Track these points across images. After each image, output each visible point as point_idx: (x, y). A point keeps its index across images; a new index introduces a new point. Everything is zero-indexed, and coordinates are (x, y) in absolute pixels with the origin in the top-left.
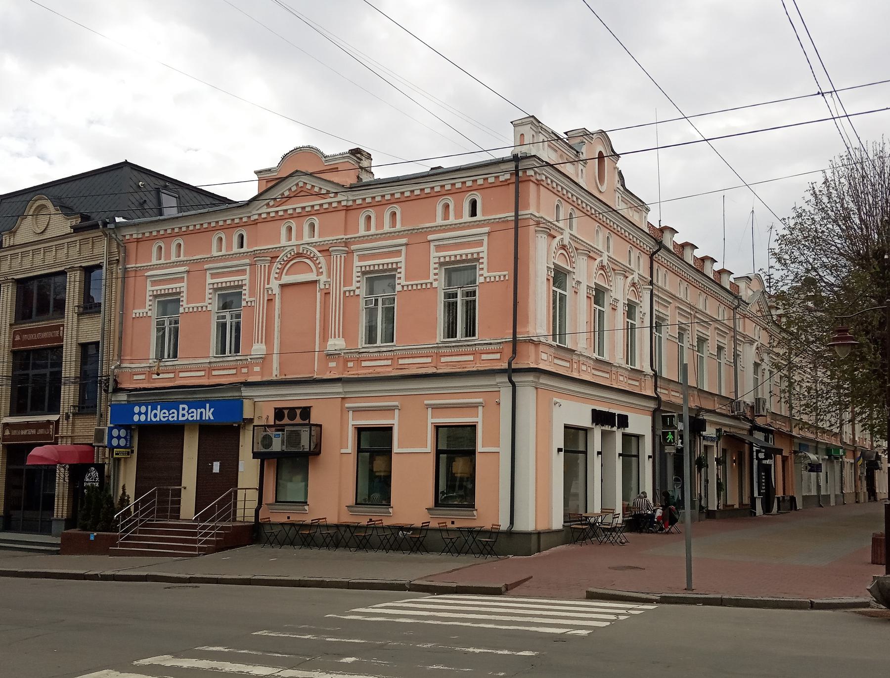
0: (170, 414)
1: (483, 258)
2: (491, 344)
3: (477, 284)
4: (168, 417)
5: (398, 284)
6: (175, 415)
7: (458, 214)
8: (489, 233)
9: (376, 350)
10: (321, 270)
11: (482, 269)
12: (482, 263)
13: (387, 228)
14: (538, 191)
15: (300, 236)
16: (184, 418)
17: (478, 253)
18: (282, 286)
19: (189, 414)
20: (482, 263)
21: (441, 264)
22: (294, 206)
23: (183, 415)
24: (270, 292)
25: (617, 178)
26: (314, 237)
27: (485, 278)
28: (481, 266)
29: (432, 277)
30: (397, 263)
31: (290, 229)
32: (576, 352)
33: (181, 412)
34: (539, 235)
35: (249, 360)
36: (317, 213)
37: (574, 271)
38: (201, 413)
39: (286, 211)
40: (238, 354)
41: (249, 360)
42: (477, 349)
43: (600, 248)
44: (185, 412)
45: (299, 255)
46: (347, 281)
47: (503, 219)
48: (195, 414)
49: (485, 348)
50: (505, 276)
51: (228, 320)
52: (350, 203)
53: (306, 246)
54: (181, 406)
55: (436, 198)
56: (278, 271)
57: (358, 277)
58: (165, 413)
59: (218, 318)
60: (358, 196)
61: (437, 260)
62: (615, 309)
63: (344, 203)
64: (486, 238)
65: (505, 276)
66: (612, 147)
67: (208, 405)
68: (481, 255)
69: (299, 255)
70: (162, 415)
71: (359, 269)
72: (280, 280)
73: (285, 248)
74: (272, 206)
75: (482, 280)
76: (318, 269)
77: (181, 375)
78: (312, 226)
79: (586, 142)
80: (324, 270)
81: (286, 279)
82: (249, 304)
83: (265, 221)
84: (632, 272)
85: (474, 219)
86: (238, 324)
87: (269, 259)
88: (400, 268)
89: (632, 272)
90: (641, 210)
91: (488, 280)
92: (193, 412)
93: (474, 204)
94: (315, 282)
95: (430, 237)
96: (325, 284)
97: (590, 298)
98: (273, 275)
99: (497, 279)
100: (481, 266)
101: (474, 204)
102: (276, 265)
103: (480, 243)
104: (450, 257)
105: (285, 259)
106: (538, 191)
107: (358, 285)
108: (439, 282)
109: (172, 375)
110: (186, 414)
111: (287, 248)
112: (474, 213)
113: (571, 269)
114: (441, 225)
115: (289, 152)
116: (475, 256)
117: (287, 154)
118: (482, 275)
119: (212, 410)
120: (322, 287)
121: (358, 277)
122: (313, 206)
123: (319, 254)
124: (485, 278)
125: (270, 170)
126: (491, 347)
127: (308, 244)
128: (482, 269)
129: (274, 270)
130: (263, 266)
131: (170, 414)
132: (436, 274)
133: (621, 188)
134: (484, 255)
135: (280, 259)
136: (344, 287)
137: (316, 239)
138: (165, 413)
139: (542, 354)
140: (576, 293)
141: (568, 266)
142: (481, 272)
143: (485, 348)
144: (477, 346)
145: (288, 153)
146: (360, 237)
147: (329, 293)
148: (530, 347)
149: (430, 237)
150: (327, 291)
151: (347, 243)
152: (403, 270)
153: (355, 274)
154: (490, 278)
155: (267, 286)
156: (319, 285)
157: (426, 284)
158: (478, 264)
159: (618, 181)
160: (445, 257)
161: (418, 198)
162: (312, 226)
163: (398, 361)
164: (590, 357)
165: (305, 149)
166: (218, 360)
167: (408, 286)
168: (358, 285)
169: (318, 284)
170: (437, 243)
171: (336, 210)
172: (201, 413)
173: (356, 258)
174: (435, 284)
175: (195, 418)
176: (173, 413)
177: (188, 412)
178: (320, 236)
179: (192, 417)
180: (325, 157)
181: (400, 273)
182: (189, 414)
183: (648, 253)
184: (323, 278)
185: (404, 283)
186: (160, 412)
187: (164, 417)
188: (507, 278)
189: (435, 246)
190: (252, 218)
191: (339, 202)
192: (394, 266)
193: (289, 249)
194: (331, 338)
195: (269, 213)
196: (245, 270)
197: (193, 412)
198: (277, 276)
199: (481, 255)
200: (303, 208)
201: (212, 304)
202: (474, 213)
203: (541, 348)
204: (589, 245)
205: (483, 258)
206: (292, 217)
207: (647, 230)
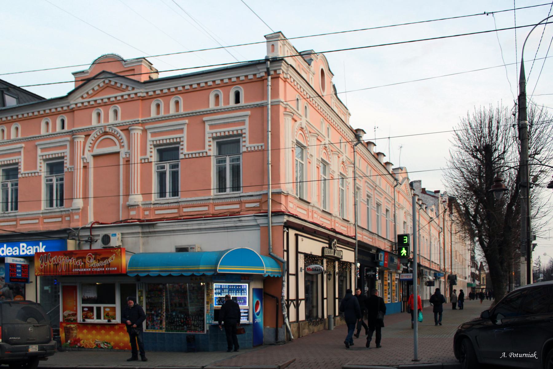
0: (13, 250)
1: (245, 133)
2: (252, 196)
4: (12, 252)
5: (182, 153)
6: (18, 251)
10: (122, 144)
11: (245, 141)
12: (245, 137)
13: (172, 111)
14: (285, 86)
15: (107, 119)
16: (24, 253)
17: (241, 130)
18: (95, 156)
19: (27, 250)
20: (245, 137)
21: (214, 139)
23: (23, 251)
28: (244, 139)
29: (207, 148)
30: (180, 138)
31: (99, 115)
33: (22, 249)
35: (71, 211)
36: (119, 102)
38: (36, 249)
39: (95, 101)
40: (62, 207)
41: (71, 211)
42: (242, 200)
44: (24, 249)
45: (106, 133)
48: (31, 250)
50: (262, 146)
51: (54, 182)
52: (145, 94)
54: (21, 245)
55: (209, 90)
56: (91, 145)
58: (9, 250)
59: (47, 181)
60: (150, 89)
61: (211, 135)
67: (41, 244)
68: (244, 131)
69: (106, 133)
70: (8, 251)
71: (152, 143)
72: (92, 152)
75: (244, 149)
76: (120, 143)
77: (22, 222)
78: (116, 112)
80: (125, 143)
82: (70, 171)
83: (80, 109)
85: (238, 105)
86: (62, 185)
87: (84, 136)
91: (249, 149)
92: (30, 249)
93: (237, 95)
94: (118, 153)
95: (205, 118)
96: (126, 155)
98: (87, 148)
99: (256, 148)
100: (244, 139)
101: (237, 95)
102: (90, 140)
103: (243, 123)
104: (220, 133)
105: (96, 136)
106: (285, 86)
108: (212, 150)
109: (14, 223)
110: (26, 250)
114: (213, 109)
116: (239, 132)
118: (245, 146)
119: (44, 247)
120: (124, 156)
122: (116, 97)
123: (121, 133)
126: (252, 198)
128: (245, 141)
129: (88, 145)
130: (79, 142)
131: (13, 250)
135: (92, 136)
137: (119, 120)
138: (9, 250)
142: (244, 144)
144: (242, 198)
149: (205, 118)
150: (127, 159)
151: (143, 123)
152: (185, 143)
154: (251, 148)
155: (82, 156)
157: (203, 153)
158: (241, 138)
160: (216, 133)
161: (195, 90)
162: (116, 112)
166: (47, 211)
167: (188, 154)
170: (210, 123)
171: (133, 100)
172: (36, 249)
173: (149, 135)
175: (32, 253)
176: (16, 249)
177: (26, 248)
179: (30, 252)
182: (27, 250)
185: (185, 151)
186: (7, 248)
187: (9, 253)
188: (263, 148)
189: (209, 125)
190: (71, 107)
192: (178, 140)
196: (66, 146)
197: (30, 249)
198: (90, 149)
200: (109, 99)
201: (42, 169)
205: (245, 133)
206: (100, 105)
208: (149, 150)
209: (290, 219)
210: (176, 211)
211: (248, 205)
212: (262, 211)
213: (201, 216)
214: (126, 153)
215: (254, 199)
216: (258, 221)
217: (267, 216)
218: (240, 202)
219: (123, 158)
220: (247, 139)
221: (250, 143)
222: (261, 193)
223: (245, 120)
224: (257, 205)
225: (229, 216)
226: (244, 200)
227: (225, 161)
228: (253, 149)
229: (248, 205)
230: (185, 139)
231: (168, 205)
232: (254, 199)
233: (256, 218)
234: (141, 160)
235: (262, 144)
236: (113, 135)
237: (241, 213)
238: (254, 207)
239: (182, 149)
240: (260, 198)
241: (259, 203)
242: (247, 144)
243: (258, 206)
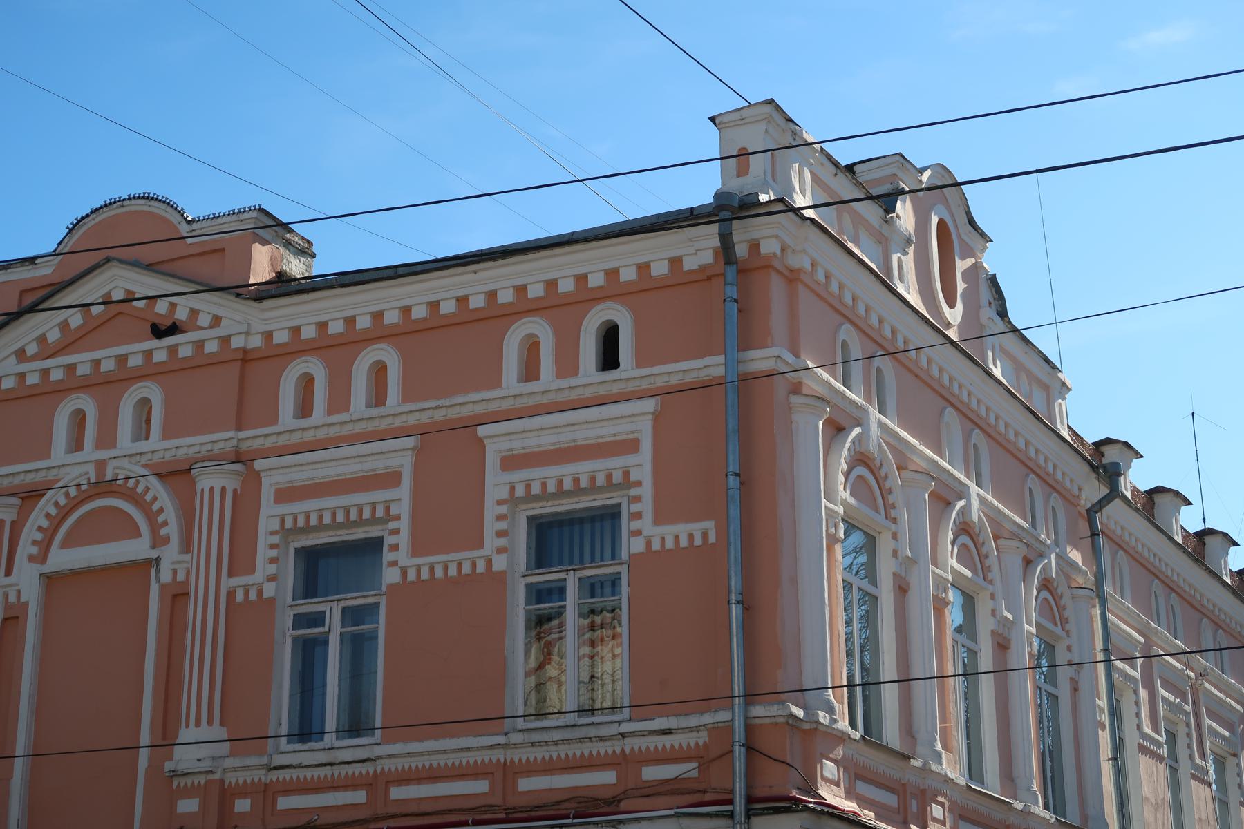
2: (668, 732)
7: (567, 366)
9: (322, 757)
11: (637, 516)
15: (107, 438)
18: (51, 581)
20: (638, 499)
22: (96, 355)
24: (12, 599)
26: (147, 438)
28: (635, 508)
39: (71, 368)
46: (240, 560)
52: (255, 342)
53: (124, 463)
56: (39, 536)
57: (272, 546)
63: (237, 343)
66: (968, 212)
68: (634, 477)
69: (102, 487)
73: (63, 470)
74: (34, 358)
75: (637, 546)
76: (155, 528)
80: (172, 530)
81: (62, 559)
85: (613, 374)
88: (398, 518)
91: (656, 546)
93: (610, 337)
95: (482, 431)
98: (26, 548)
100: (635, 508)
101: (610, 337)
102: (37, 519)
107: (272, 569)
111: (68, 469)
112: (609, 358)
115: (89, 211)
117: (83, 218)
118: (638, 533)
121: (272, 546)
125: (32, 260)
127: (130, 456)
128: (637, 516)
129: (30, 534)
132: (500, 534)
135: (48, 501)
136: (231, 574)
141: (878, 512)
142: (635, 525)
145: (87, 216)
146: (279, 434)
147: (187, 594)
153: (263, 541)
156: (158, 571)
159: (990, 303)
163: (387, 793)
165: (133, 202)
168: (272, 569)
169: (153, 571)
174: (500, 563)
178: (167, 435)
180: (189, 222)
181: (396, 532)
184: (170, 555)
191: (225, 340)
193: (77, 470)
194: (187, 726)
195: (22, 376)
202: (609, 358)
208: (263, 553)
210: (360, 797)
212: (708, 797)
213: (462, 818)
214: (173, 563)
217: (730, 815)
219: (163, 587)
220: (646, 507)
225: (574, 818)
227: (559, 591)
229: (651, 773)
230: (403, 509)
231: (327, 771)
234: (231, 594)
235: (709, 525)
236: (131, 496)
237: (623, 805)
239: (395, 548)
241: (695, 764)
243: (695, 774)
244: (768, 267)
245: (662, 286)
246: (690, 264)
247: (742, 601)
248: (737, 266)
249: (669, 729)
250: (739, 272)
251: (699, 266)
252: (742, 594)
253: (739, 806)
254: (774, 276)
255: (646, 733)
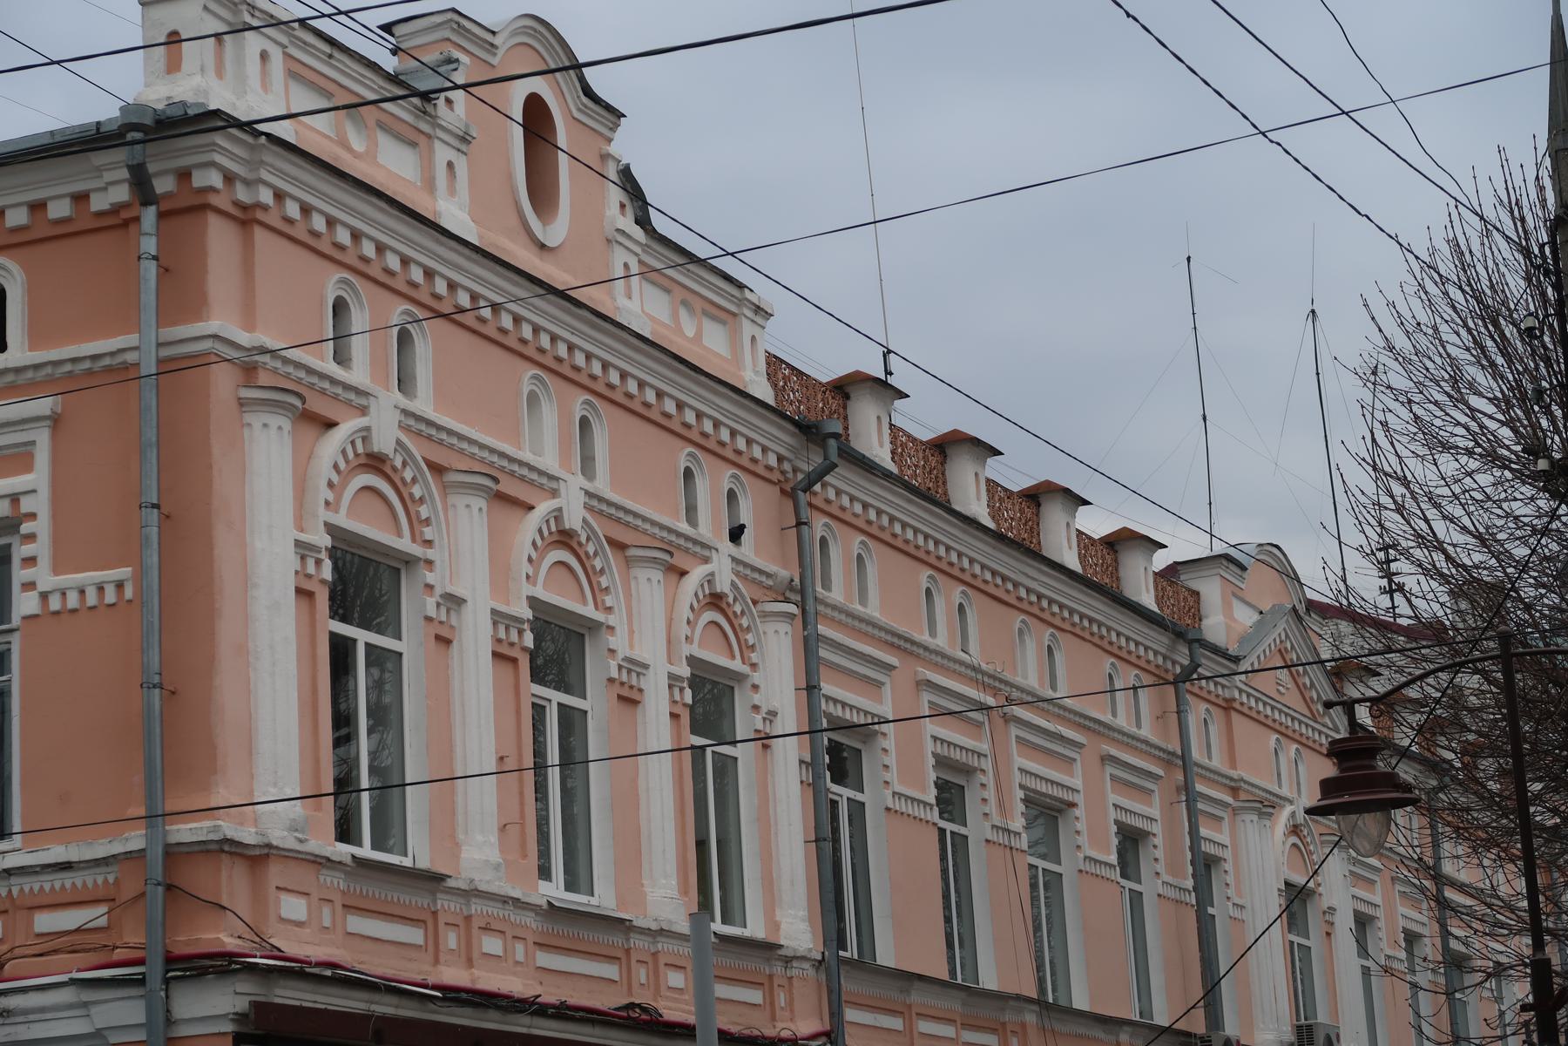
2: (66, 866)
3: (16, 621)
8: (55, 421)
11: (30, 561)
14: (248, 246)
20: (31, 537)
25: (616, 195)
27: (44, 596)
28: (27, 550)
32: (451, 883)
34: (256, 419)
37: (430, 554)
42: (15, 891)
43: (549, 460)
47: (107, 361)
49: (47, 887)
50: (120, 586)
62: (634, 703)
64: (42, 438)
65: (120, 586)
68: (26, 505)
79: (464, 58)
84: (706, 553)
89: (706, 553)
90: (734, 315)
91: (55, 604)
97: (514, 661)
99: (92, 599)
100: (27, 550)
106: (248, 246)
113: (416, 550)
124: (44, 596)
128: (30, 561)
133: (638, 233)
134: (39, 504)
139: (284, 897)
140: (444, 641)
141: (400, 535)
143: (47, 887)
144: (14, 880)
148: (224, 874)
154: (64, 594)
158: (14, 541)
159: (623, 206)
164: (518, 900)
183: (775, 476)
188: (129, 593)
199: (26, 505)
203: (276, 873)
204: (492, 451)
205: (32, 516)
207: (765, 392)
209: (279, 992)
211: (46, 922)
212: (119, 954)
215: (79, 884)
216: (94, 1010)
217: (140, 981)
218: (8, 906)
220: (41, 548)
221: (56, 570)
222: (117, 848)
223: (33, 443)
224: (93, 915)
226: (27, 889)
228: (73, 600)
229: (46, 922)
232: (79, 884)
233: (88, 995)
235: (123, 572)
238: (78, 930)
240: (111, 879)
241: (103, 909)
242: (46, 578)
243: (103, 922)
244: (205, 207)
245: (64, 233)
246: (98, 203)
247: (161, 684)
248: (158, 208)
249: (69, 863)
250: (161, 215)
251: (111, 204)
252: (160, 674)
253: (154, 970)
254: (214, 221)
255: (38, 869)
